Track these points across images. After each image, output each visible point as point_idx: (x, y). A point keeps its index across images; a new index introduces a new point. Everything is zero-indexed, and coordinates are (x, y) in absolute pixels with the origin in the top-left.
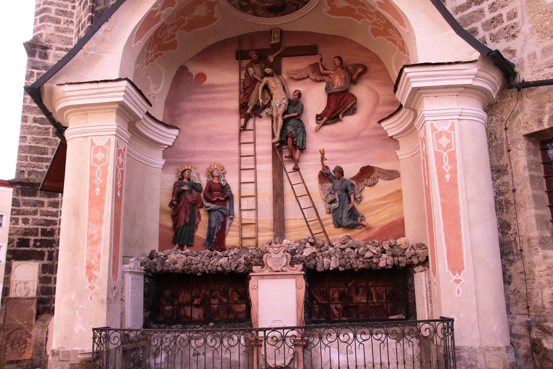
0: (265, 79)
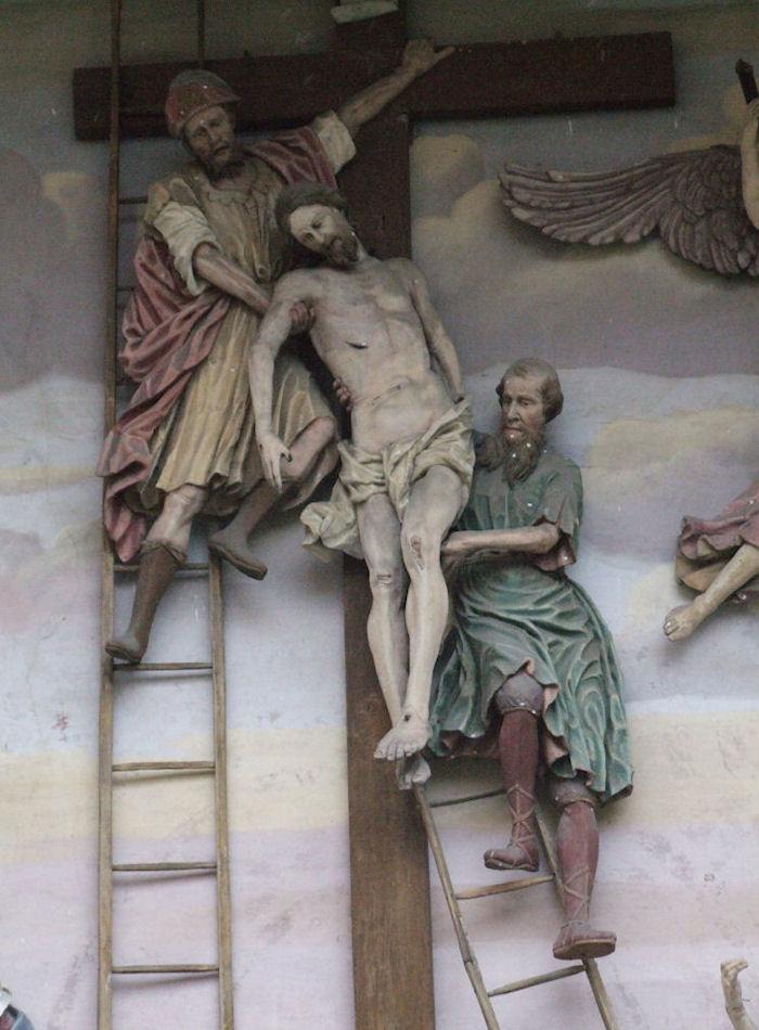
0: (297, 285)
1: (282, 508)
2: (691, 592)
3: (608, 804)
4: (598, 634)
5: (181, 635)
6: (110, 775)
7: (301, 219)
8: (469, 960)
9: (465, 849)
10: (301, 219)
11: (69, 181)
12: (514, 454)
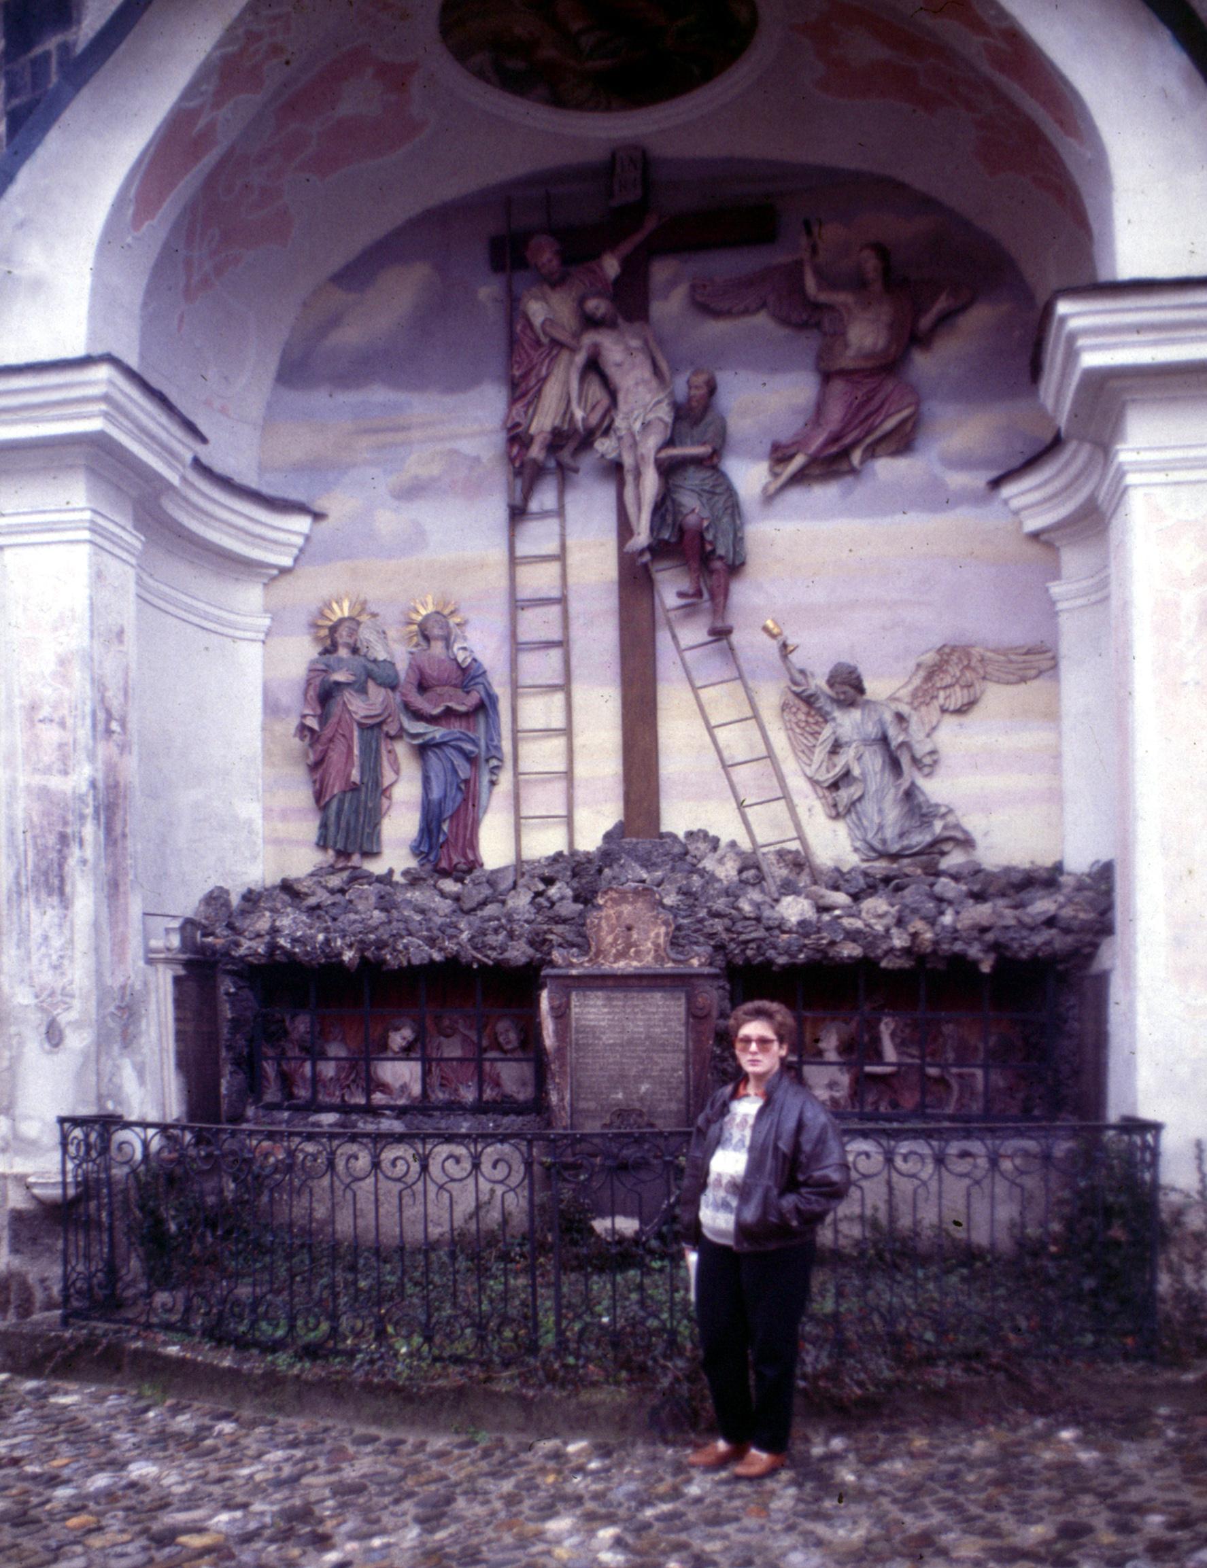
1: (586, 440)
2: (776, 475)
3: (735, 568)
4: (731, 492)
5: (545, 498)
6: (514, 561)
7: (591, 304)
8: (674, 637)
9: (670, 588)
10: (591, 304)
11: (488, 291)
12: (695, 414)
